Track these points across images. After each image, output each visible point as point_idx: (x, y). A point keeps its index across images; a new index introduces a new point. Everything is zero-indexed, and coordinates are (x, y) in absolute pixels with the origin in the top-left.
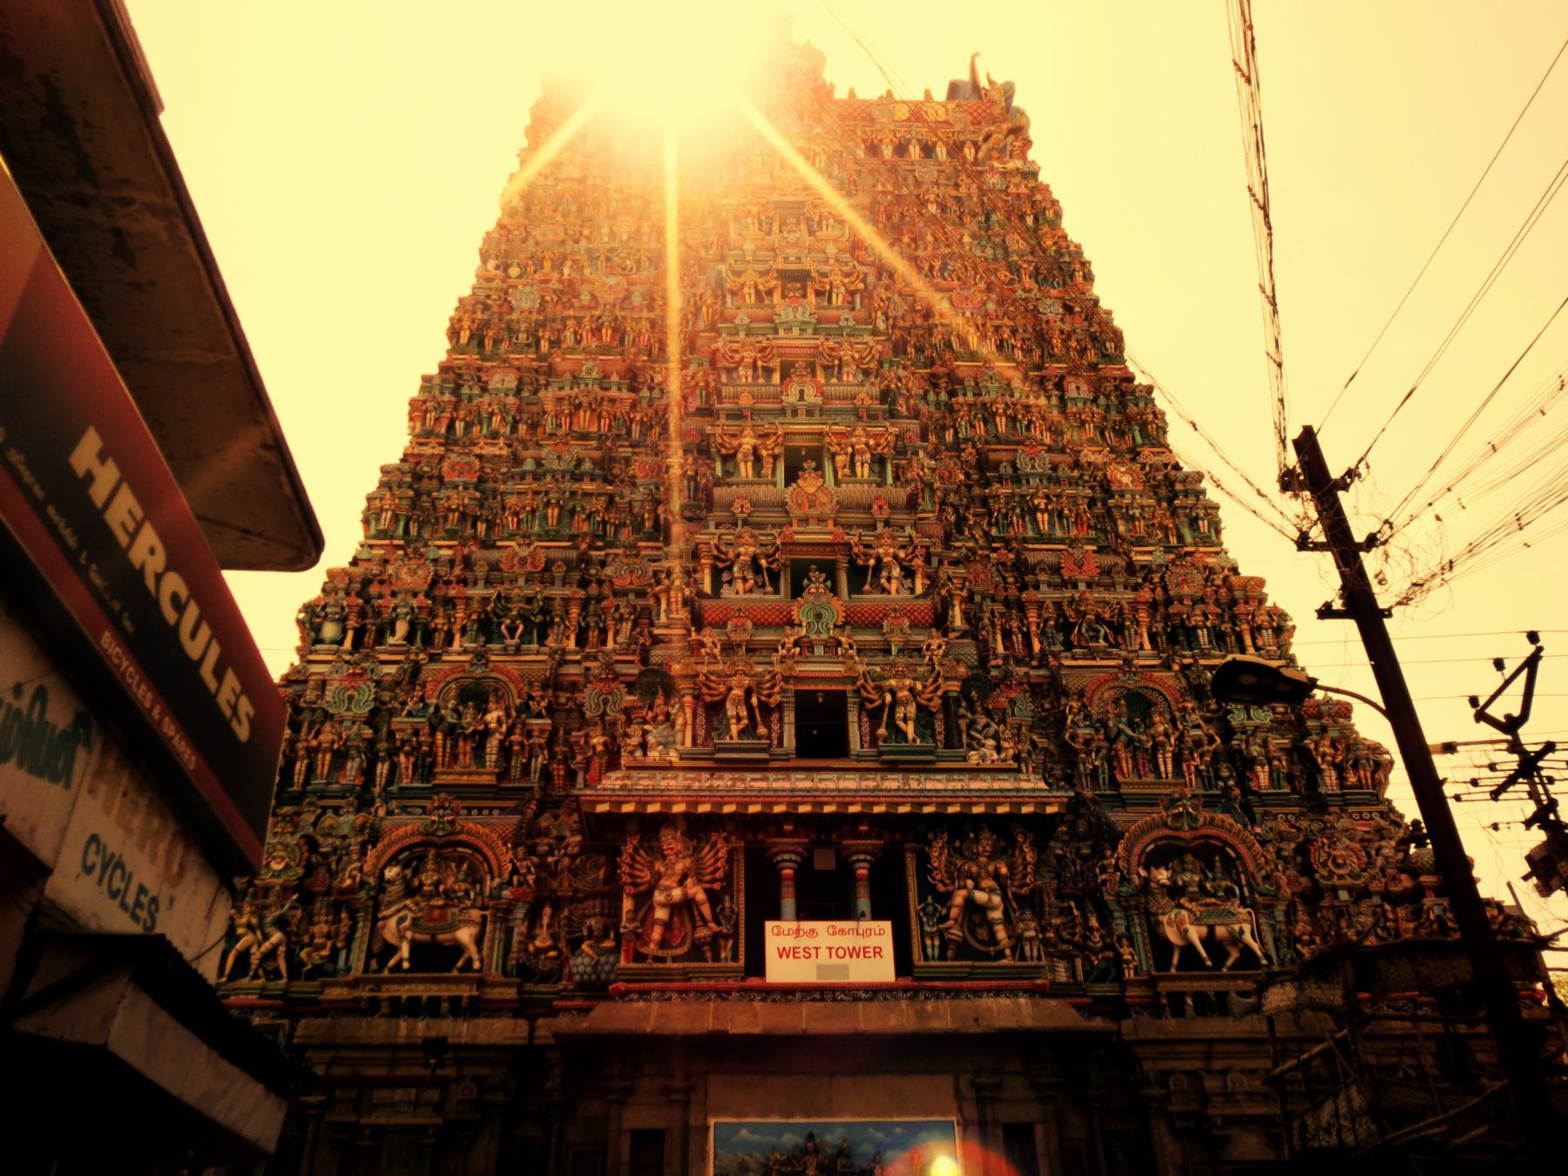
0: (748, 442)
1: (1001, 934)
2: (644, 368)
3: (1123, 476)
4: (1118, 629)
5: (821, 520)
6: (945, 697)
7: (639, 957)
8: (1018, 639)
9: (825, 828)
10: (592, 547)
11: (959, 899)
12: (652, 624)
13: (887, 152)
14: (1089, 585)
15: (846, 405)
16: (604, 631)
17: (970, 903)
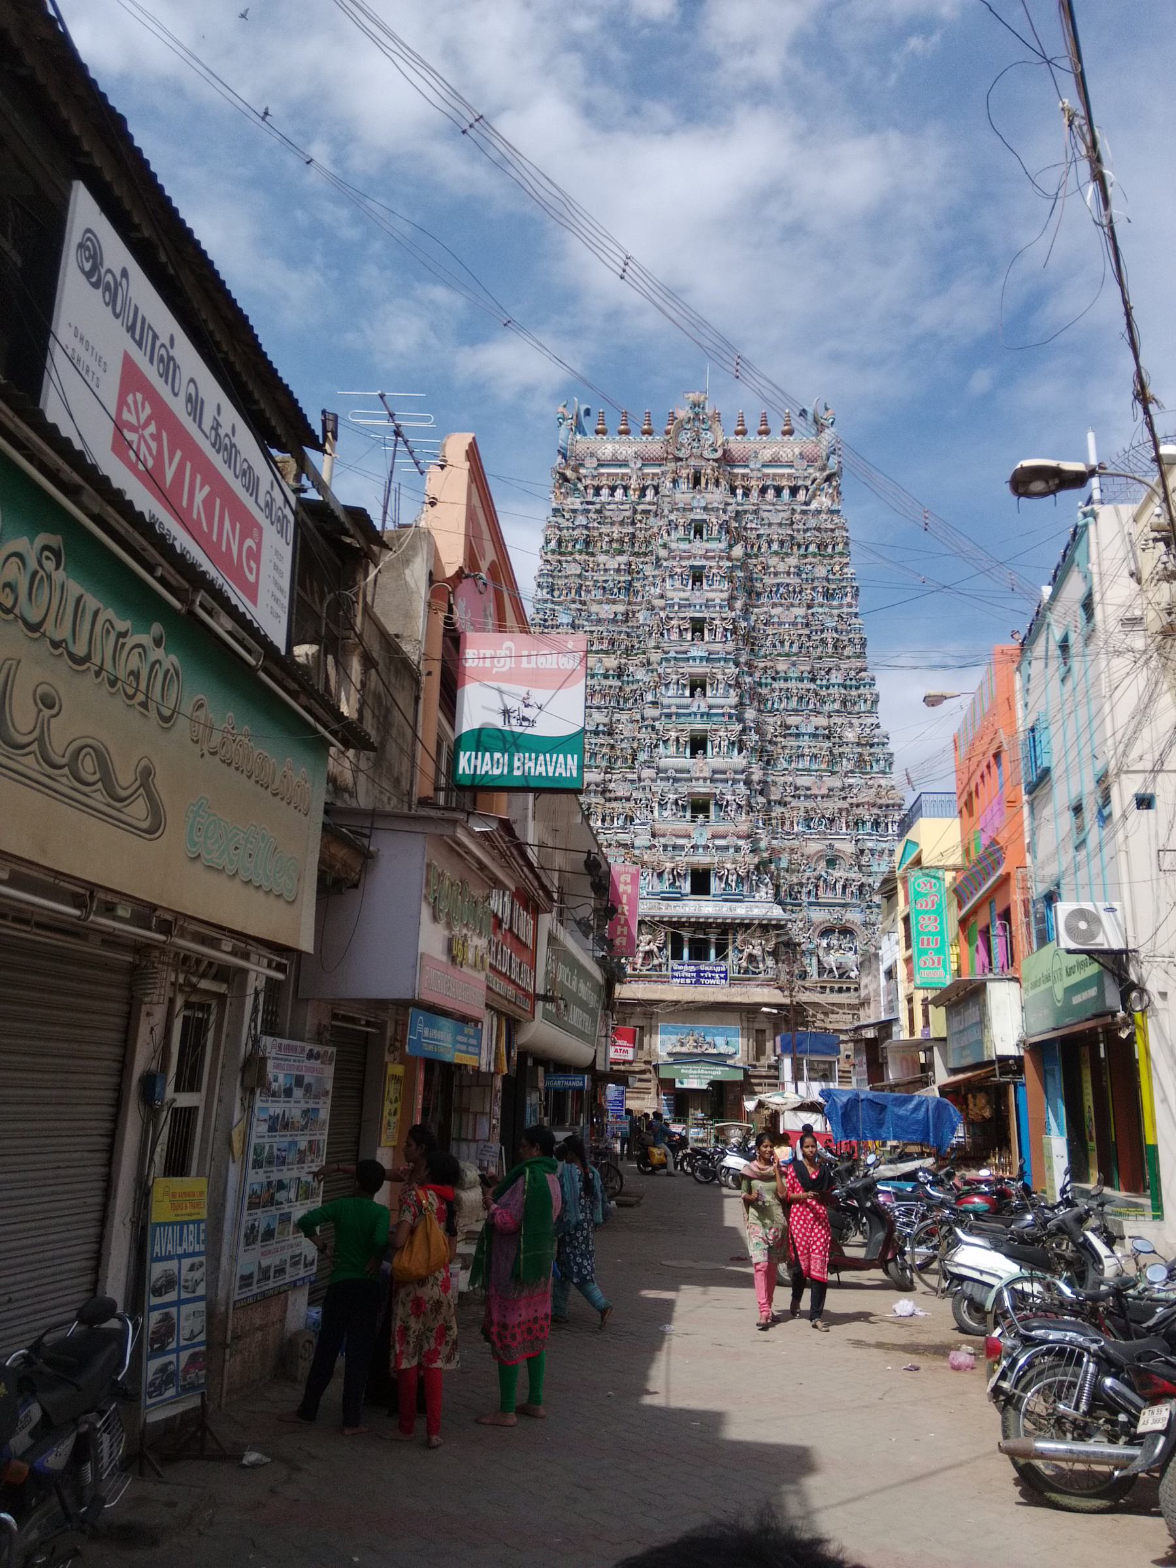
0: (673, 734)
1: (761, 965)
2: (625, 664)
3: (850, 735)
4: (832, 821)
5: (705, 779)
7: (634, 969)
8: (788, 823)
9: (701, 925)
11: (745, 954)
12: (632, 820)
13: (755, 493)
17: (750, 955)
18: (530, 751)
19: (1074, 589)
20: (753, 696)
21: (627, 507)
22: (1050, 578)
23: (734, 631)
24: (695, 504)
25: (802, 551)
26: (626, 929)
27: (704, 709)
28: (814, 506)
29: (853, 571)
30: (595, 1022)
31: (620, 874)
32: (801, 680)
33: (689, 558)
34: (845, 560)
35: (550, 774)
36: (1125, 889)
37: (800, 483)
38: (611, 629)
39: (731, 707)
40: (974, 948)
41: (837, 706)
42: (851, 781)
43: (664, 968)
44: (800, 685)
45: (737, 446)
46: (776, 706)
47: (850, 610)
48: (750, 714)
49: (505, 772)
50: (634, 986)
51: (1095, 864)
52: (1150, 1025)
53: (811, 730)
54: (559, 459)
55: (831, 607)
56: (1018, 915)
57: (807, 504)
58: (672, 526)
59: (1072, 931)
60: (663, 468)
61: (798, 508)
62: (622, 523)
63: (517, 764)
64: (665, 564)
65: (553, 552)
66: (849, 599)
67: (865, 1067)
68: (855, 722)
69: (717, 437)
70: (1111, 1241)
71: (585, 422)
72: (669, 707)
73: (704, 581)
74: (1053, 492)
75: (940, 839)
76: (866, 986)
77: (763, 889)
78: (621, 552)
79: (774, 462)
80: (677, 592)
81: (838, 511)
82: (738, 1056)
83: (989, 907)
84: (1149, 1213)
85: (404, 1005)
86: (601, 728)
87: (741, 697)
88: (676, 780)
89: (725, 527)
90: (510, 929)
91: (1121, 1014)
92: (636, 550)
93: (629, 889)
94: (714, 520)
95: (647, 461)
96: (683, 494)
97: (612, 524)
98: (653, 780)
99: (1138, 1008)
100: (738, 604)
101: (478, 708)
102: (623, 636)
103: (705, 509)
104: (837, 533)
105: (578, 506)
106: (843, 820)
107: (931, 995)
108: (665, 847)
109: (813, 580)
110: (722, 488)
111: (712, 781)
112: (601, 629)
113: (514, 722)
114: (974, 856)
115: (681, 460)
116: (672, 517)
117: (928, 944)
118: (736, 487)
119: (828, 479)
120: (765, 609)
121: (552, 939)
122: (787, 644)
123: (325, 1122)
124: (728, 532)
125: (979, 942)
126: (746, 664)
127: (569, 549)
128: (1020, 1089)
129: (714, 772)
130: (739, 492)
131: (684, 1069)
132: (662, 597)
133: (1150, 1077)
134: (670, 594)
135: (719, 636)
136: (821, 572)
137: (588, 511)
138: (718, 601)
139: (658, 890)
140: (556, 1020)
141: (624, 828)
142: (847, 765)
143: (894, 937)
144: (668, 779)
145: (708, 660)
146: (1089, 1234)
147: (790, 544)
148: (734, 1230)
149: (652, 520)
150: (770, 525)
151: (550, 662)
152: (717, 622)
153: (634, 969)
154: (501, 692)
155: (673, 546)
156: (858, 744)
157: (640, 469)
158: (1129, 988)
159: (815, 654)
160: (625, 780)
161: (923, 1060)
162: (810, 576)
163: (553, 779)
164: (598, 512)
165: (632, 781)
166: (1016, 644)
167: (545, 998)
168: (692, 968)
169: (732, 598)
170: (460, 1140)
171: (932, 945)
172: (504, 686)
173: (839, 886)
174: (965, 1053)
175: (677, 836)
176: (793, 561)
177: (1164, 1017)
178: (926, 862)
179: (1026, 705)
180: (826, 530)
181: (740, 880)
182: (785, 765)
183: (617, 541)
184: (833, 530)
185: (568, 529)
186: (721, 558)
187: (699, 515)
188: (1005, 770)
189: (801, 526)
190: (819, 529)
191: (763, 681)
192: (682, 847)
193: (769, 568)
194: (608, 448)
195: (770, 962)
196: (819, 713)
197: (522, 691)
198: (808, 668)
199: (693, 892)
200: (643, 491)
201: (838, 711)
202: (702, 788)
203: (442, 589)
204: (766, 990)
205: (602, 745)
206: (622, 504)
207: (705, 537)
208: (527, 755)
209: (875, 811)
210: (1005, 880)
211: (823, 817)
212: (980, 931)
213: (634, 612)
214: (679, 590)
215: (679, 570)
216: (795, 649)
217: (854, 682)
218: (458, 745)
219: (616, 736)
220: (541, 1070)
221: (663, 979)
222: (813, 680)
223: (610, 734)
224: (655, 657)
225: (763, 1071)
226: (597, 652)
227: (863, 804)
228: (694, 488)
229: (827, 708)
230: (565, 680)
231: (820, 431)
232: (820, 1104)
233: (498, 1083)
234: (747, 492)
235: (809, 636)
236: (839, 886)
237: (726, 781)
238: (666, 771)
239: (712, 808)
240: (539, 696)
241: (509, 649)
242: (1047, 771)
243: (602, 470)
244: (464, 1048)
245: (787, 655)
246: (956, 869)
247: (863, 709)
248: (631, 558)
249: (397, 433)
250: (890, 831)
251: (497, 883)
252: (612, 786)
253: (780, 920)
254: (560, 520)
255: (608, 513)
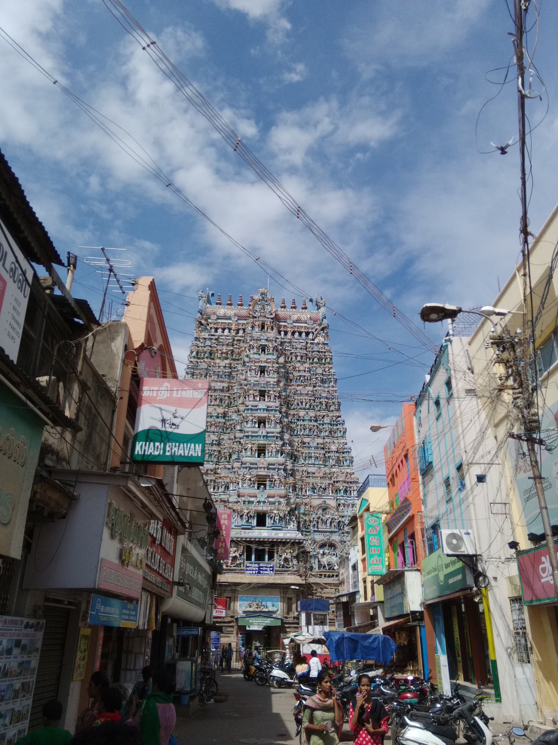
0: (250, 446)
1: (290, 564)
2: (227, 412)
3: (333, 448)
4: (325, 489)
5: (264, 468)
6: (285, 515)
8: (304, 490)
9: (261, 542)
10: (216, 464)
12: (228, 488)
14: (321, 478)
15: (272, 435)
16: (218, 487)
18: (176, 441)
19: (441, 377)
20: (288, 428)
21: (230, 338)
22: (429, 371)
23: (279, 397)
24: (262, 338)
25: (311, 361)
26: (224, 544)
27: (264, 434)
28: (316, 341)
29: (334, 371)
30: (205, 596)
31: (222, 514)
32: (311, 421)
33: (259, 362)
34: (330, 366)
35: (186, 455)
36: (474, 522)
37: (310, 330)
38: (221, 394)
39: (277, 433)
40: (396, 553)
41: (327, 434)
42: (334, 470)
43: (242, 566)
44: (310, 423)
45: (282, 313)
46: (299, 433)
47: (333, 389)
48: (286, 436)
49: (161, 453)
50: (227, 575)
51: (457, 512)
52: (489, 593)
53: (315, 445)
54: (199, 315)
55: (324, 387)
56: (418, 536)
57: (313, 340)
58: (251, 347)
59: (449, 544)
60: (247, 321)
61: (309, 342)
62: (227, 345)
63: (168, 448)
64: (247, 364)
65: (194, 357)
66: (332, 384)
67: (342, 618)
68: (336, 441)
69: (273, 308)
70: (486, 720)
71: (212, 299)
72: (248, 432)
73: (266, 373)
74: (441, 320)
75: (378, 498)
76: (342, 574)
77: (292, 523)
78: (226, 358)
79: (298, 321)
80: (253, 377)
81: (327, 344)
82: (279, 612)
83: (404, 533)
84: (494, 698)
85: (90, 591)
86: (214, 442)
87: (282, 428)
88: (250, 468)
89: (275, 349)
90: (160, 544)
91: (475, 589)
92: (234, 357)
93: (226, 522)
94: (271, 345)
95: (240, 318)
96: (257, 332)
97: (223, 345)
98: (239, 468)
99: (483, 586)
100: (282, 384)
101: (148, 418)
102: (226, 398)
103: (267, 340)
104: (326, 354)
105: (207, 336)
106: (330, 489)
107: (376, 579)
108: (244, 502)
109: (316, 375)
110: (274, 331)
111: (268, 469)
112: (216, 394)
113: (167, 426)
114: (396, 507)
115: (256, 317)
116: (251, 343)
117: (374, 552)
118: (281, 331)
119: (323, 329)
120: (294, 387)
121: (184, 550)
122: (304, 404)
123: (34, 669)
124: (277, 351)
125: (399, 551)
126: (285, 412)
127: (202, 356)
128: (422, 629)
129: (269, 464)
130: (282, 333)
131: (251, 620)
132: (246, 380)
133: (491, 623)
134: (249, 379)
135: (272, 399)
136: (320, 371)
137: (212, 339)
138: (272, 383)
139: (240, 524)
140: (185, 596)
141: (224, 492)
142: (332, 462)
143: (356, 548)
144: (246, 468)
145: (267, 410)
146: (477, 718)
147: (305, 358)
148: (278, 715)
149: (242, 344)
150: (296, 348)
151: (189, 394)
152: (271, 392)
153: (227, 566)
154: (161, 409)
155: (252, 356)
156: (337, 452)
157: (237, 321)
158: (478, 575)
159: (317, 409)
160: (225, 468)
161: (372, 613)
162: (314, 373)
163: (188, 457)
164: (216, 339)
165: (229, 469)
166: (413, 403)
167: (179, 584)
168: (257, 565)
169: (279, 381)
170: (126, 669)
171: (376, 552)
172: (163, 407)
173: (328, 522)
174: (394, 610)
175: (250, 497)
176: (307, 365)
177: (496, 590)
178: (371, 510)
179: (419, 432)
180: (322, 352)
181: (281, 519)
182: (303, 462)
183: (225, 353)
184: (325, 352)
185: (202, 347)
186: (273, 362)
187: (263, 342)
188: (410, 464)
189: (310, 349)
190: (319, 352)
191: (293, 421)
192: (253, 502)
193: (296, 368)
194: (222, 311)
195: (295, 562)
196: (319, 437)
197: (172, 409)
198: (314, 415)
199: (258, 525)
200: (238, 331)
201: (328, 436)
202: (263, 472)
203: (131, 354)
204: (293, 577)
205: (215, 451)
206: (228, 336)
207: (266, 353)
208: (174, 444)
209: (346, 485)
210: (412, 518)
211: (321, 487)
212: (400, 545)
213: (232, 387)
214: (254, 377)
215: (254, 368)
216: (308, 406)
217: (335, 422)
218: (136, 438)
219: (221, 447)
220: (175, 625)
221: (242, 572)
222: (316, 421)
223: (219, 444)
224: (242, 408)
225: (291, 620)
226: (214, 405)
227: (340, 481)
228: (262, 330)
229: (323, 434)
230: (196, 404)
231: (319, 308)
232: (323, 640)
233: (150, 635)
234: (286, 333)
235: (314, 400)
236: (328, 522)
237: (274, 469)
238: (245, 464)
239: (268, 483)
240: (182, 412)
241: (167, 387)
242: (431, 463)
243: (219, 321)
244: (127, 617)
245: (304, 409)
246: (387, 513)
247: (339, 435)
248: (232, 361)
249: (111, 270)
250: (352, 495)
251: (153, 516)
252: (219, 471)
253: (300, 540)
254: (198, 343)
255: (221, 340)
